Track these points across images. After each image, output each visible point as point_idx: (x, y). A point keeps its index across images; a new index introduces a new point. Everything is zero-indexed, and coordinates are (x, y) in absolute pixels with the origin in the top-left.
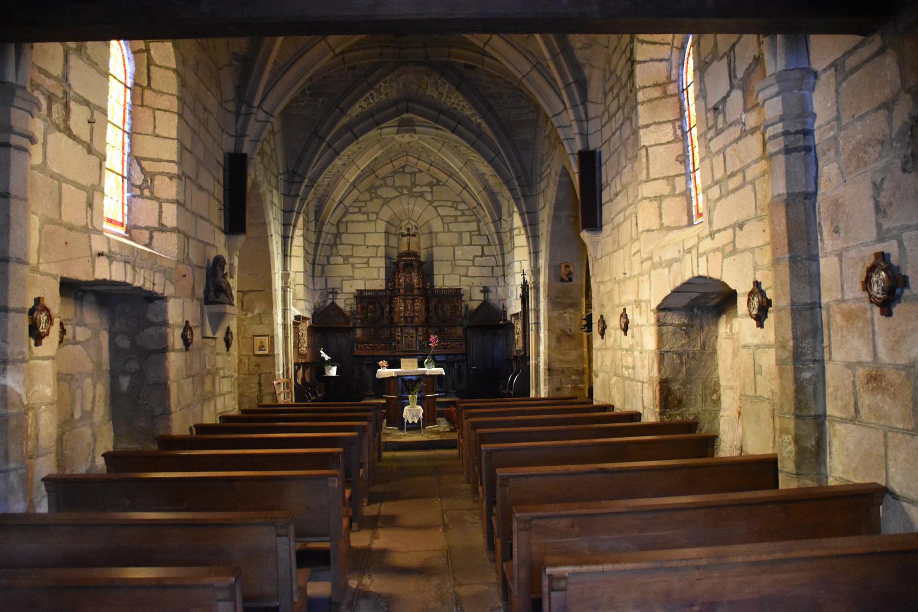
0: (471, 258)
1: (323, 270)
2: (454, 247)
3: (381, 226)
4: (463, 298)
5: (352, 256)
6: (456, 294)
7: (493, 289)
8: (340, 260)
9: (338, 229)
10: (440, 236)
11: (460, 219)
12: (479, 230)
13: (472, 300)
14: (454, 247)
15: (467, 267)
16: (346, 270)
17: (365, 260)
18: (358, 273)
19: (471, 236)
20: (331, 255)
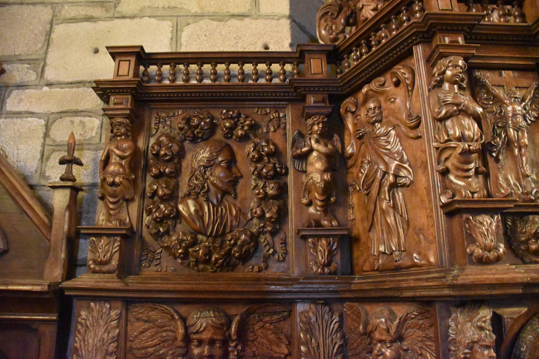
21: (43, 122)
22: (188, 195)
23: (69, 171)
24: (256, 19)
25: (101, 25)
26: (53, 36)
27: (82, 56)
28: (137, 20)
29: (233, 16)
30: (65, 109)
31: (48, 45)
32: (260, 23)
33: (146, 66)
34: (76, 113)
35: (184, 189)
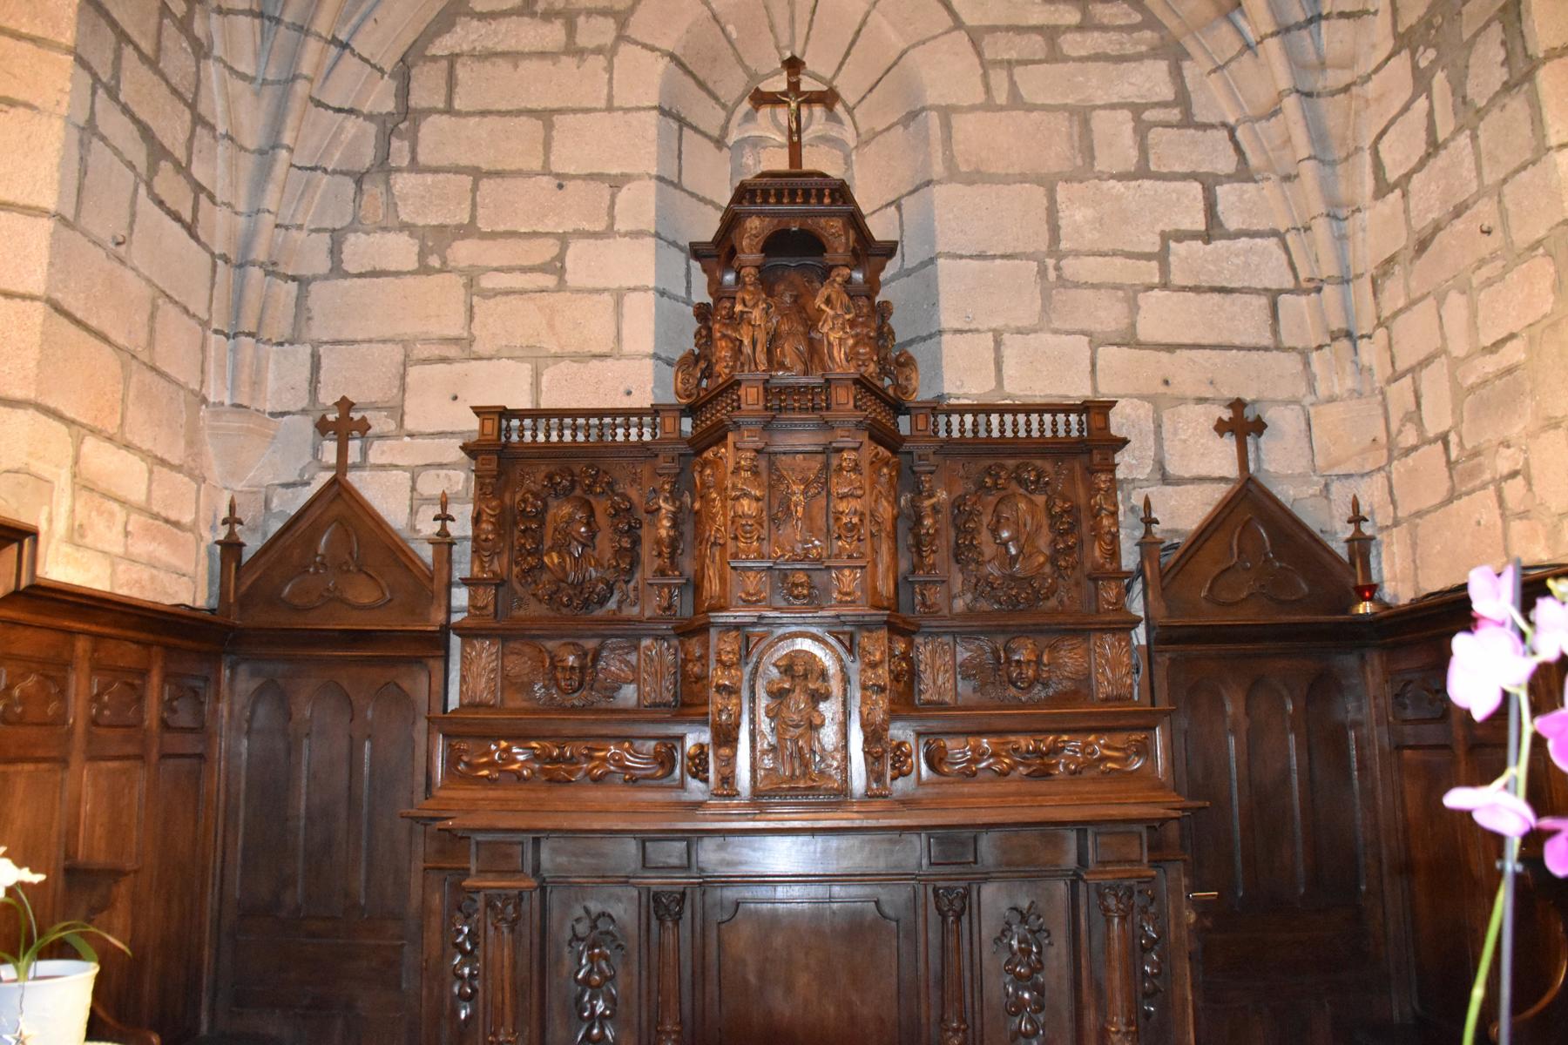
0: (1152, 244)
3: (643, 77)
4: (1123, 459)
5: (468, 230)
6: (1085, 443)
8: (400, 250)
9: (403, 92)
10: (964, 126)
11: (1071, 44)
12: (1182, 99)
13: (1166, 479)
15: (1131, 295)
16: (436, 307)
17: (545, 251)
18: (494, 322)
19: (1142, 130)
20: (355, 225)
21: (408, 475)
22: (552, 549)
23: (444, 527)
25: (457, 367)
26: (408, 379)
27: (444, 410)
28: (495, 362)
29: (595, 356)
32: (623, 362)
33: (509, 421)
34: (441, 466)
35: (548, 543)
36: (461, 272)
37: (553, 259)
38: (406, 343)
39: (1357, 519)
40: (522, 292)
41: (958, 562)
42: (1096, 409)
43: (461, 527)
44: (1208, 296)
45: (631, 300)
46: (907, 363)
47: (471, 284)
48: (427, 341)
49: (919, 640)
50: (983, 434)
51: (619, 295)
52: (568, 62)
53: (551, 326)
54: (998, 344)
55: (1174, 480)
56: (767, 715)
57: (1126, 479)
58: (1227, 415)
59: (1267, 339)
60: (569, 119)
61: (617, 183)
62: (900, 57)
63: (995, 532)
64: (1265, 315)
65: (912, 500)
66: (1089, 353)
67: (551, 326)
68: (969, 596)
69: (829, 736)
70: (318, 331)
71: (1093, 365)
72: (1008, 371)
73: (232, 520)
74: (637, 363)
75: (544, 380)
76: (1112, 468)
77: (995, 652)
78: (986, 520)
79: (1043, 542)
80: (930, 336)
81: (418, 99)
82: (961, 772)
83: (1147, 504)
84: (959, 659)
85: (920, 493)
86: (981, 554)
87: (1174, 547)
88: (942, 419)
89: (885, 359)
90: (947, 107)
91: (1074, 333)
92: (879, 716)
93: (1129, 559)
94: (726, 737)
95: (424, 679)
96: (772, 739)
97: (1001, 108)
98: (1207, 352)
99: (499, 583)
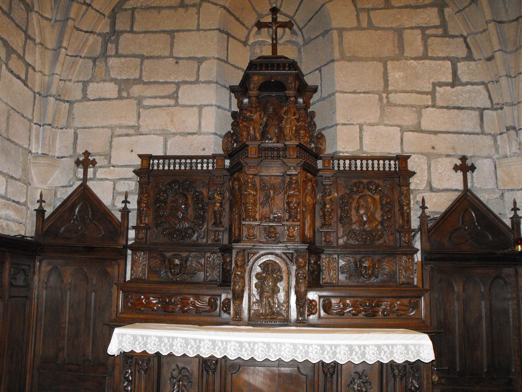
0: (428, 88)
1: (70, 112)
2: (384, 62)
5: (139, 81)
7: (484, 167)
8: (110, 89)
9: (113, 24)
12: (444, 25)
13: (432, 190)
14: (384, 62)
16: (124, 114)
17: (172, 89)
19: (425, 38)
21: (112, 183)
24: (199, 135)
25: (134, 138)
26: (113, 143)
28: (148, 136)
29: (190, 134)
30: (121, 177)
31: (111, 148)
33: (153, 161)
34: (126, 179)
36: (136, 99)
37: (174, 93)
38: (111, 128)
39: (515, 209)
40: (160, 107)
41: (341, 223)
42: (402, 159)
43: (133, 205)
44: (452, 110)
45: (205, 110)
46: (321, 137)
47: (139, 104)
48: (121, 127)
49: (323, 256)
50: (353, 168)
51: (201, 107)
52: (181, 10)
53: (172, 121)
54: (361, 130)
55: (434, 190)
56: (256, 287)
57: (414, 190)
58: (459, 163)
59: (478, 130)
60: (181, 34)
61: (200, 61)
62: (321, 7)
63: (357, 210)
64: (477, 120)
65: (322, 196)
66: (400, 135)
67: (172, 121)
68: (345, 238)
69: (281, 296)
70: (77, 123)
71: (402, 140)
72: (365, 141)
73: (41, 201)
74: (207, 137)
75: (169, 143)
76: (408, 185)
77: (355, 262)
78: (354, 205)
79: (378, 216)
80: (332, 126)
81: (119, 27)
82: (337, 313)
83: (423, 200)
84: (340, 265)
85: (326, 193)
86: (351, 220)
87: (434, 219)
88: (336, 162)
89: (312, 136)
90: (341, 28)
91: (394, 126)
92: (303, 289)
93: (415, 224)
94: (238, 297)
95: (116, 267)
96: (258, 298)
97: (364, 29)
98: (451, 135)
99: (147, 228)
